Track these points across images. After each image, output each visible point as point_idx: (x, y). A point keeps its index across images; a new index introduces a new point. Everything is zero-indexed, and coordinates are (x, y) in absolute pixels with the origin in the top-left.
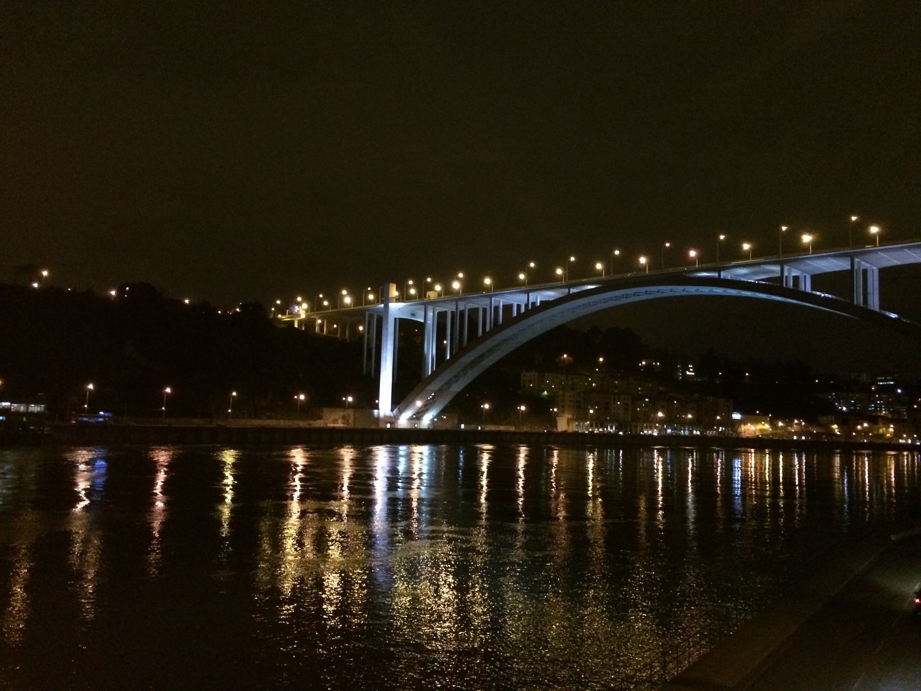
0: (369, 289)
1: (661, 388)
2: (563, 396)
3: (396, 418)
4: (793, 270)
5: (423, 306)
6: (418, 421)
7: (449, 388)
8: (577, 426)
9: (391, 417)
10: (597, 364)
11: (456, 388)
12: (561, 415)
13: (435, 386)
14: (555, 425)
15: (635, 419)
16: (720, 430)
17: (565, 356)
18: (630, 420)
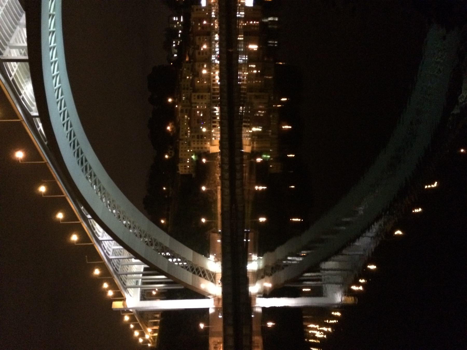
1: (187, 59)
2: (194, 148)
3: (215, 297)
4: (12, 41)
5: (128, 289)
6: (217, 274)
7: (191, 262)
8: (215, 139)
9: (215, 300)
10: (173, 103)
11: (189, 254)
12: (208, 149)
14: (215, 154)
15: (209, 89)
16: (214, 16)
17: (169, 128)
18: (209, 94)
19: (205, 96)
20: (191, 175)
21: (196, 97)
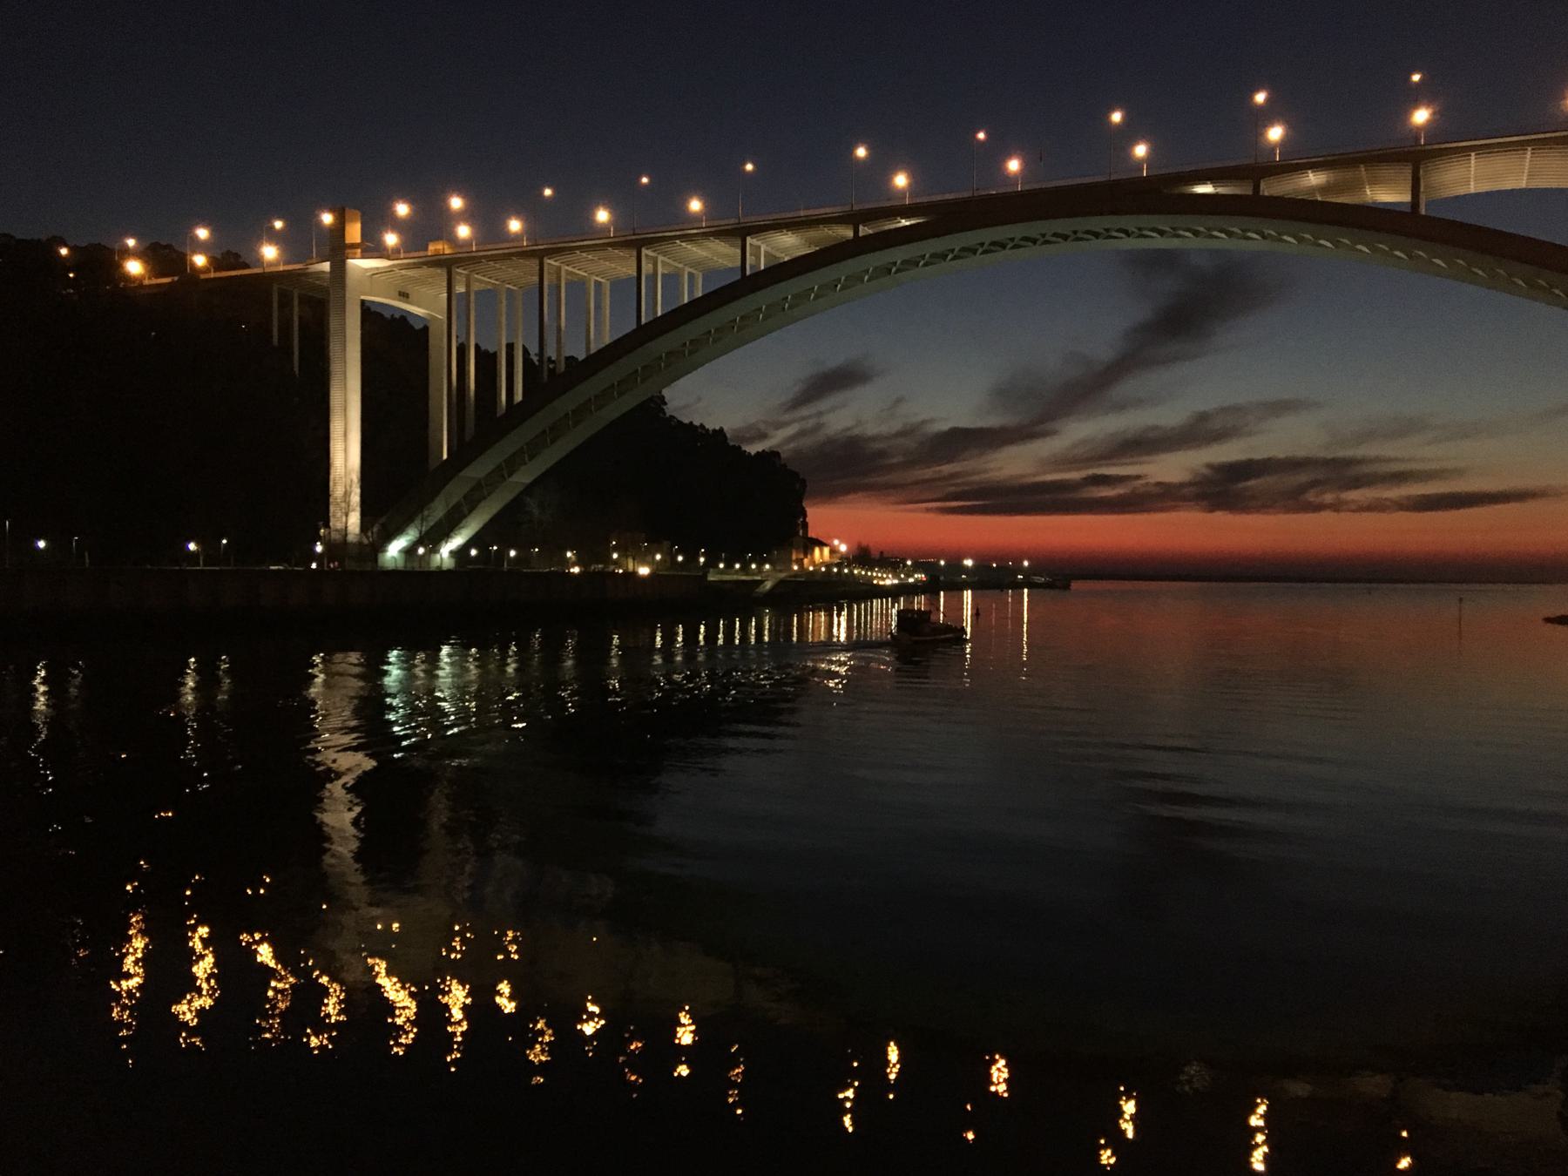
0: (278, 225)
7: (510, 475)
13: (478, 470)
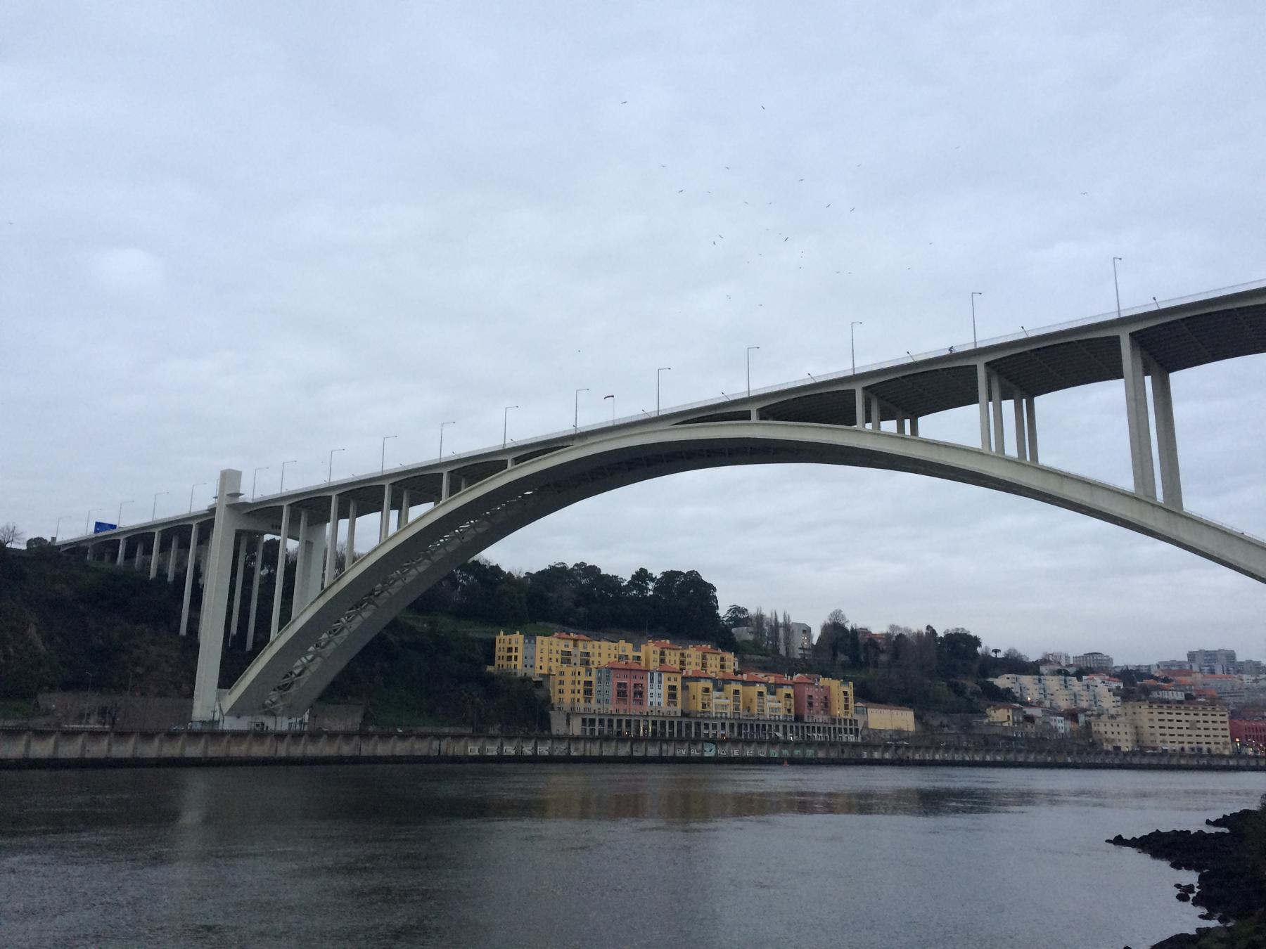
19: (675, 705)
20: (493, 664)
21: (673, 683)
